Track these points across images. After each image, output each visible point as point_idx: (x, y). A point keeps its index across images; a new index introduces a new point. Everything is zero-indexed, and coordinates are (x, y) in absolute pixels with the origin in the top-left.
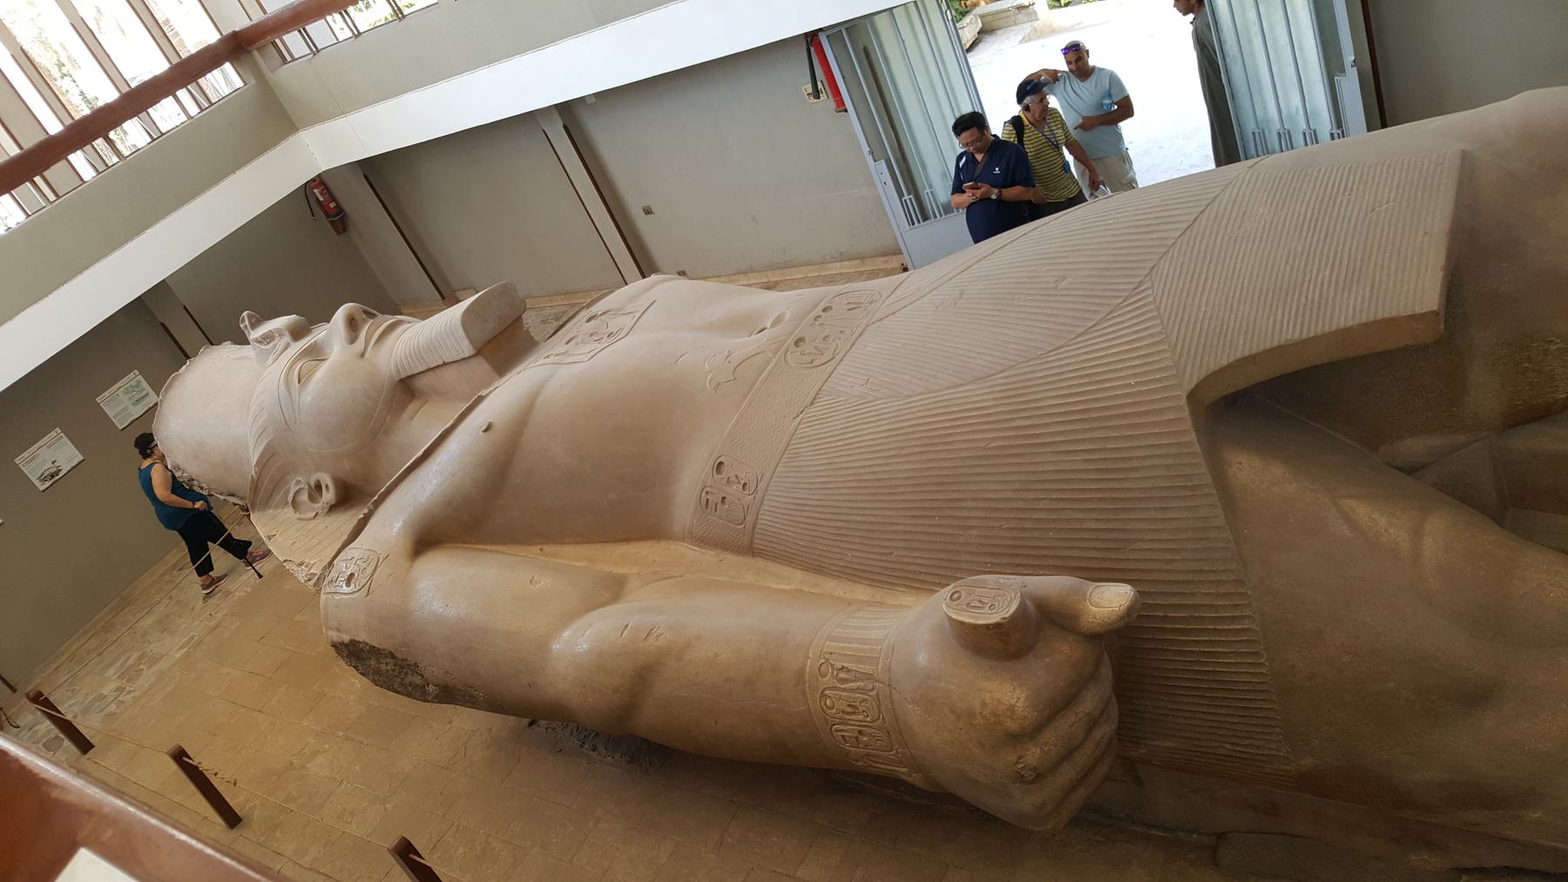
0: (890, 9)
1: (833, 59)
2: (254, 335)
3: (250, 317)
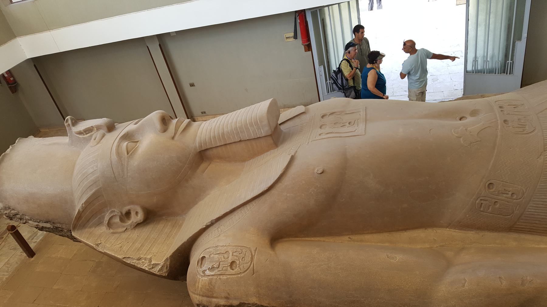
0: (339, 4)
1: (305, 25)
2: (75, 129)
3: (72, 119)
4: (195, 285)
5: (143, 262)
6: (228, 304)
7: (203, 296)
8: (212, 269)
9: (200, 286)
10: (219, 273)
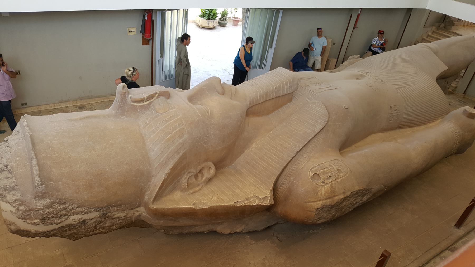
0: (178, 10)
1: (148, 22)
4: (317, 194)
5: (253, 200)
6: (346, 196)
7: (326, 199)
8: (329, 178)
9: (323, 193)
10: (335, 179)
